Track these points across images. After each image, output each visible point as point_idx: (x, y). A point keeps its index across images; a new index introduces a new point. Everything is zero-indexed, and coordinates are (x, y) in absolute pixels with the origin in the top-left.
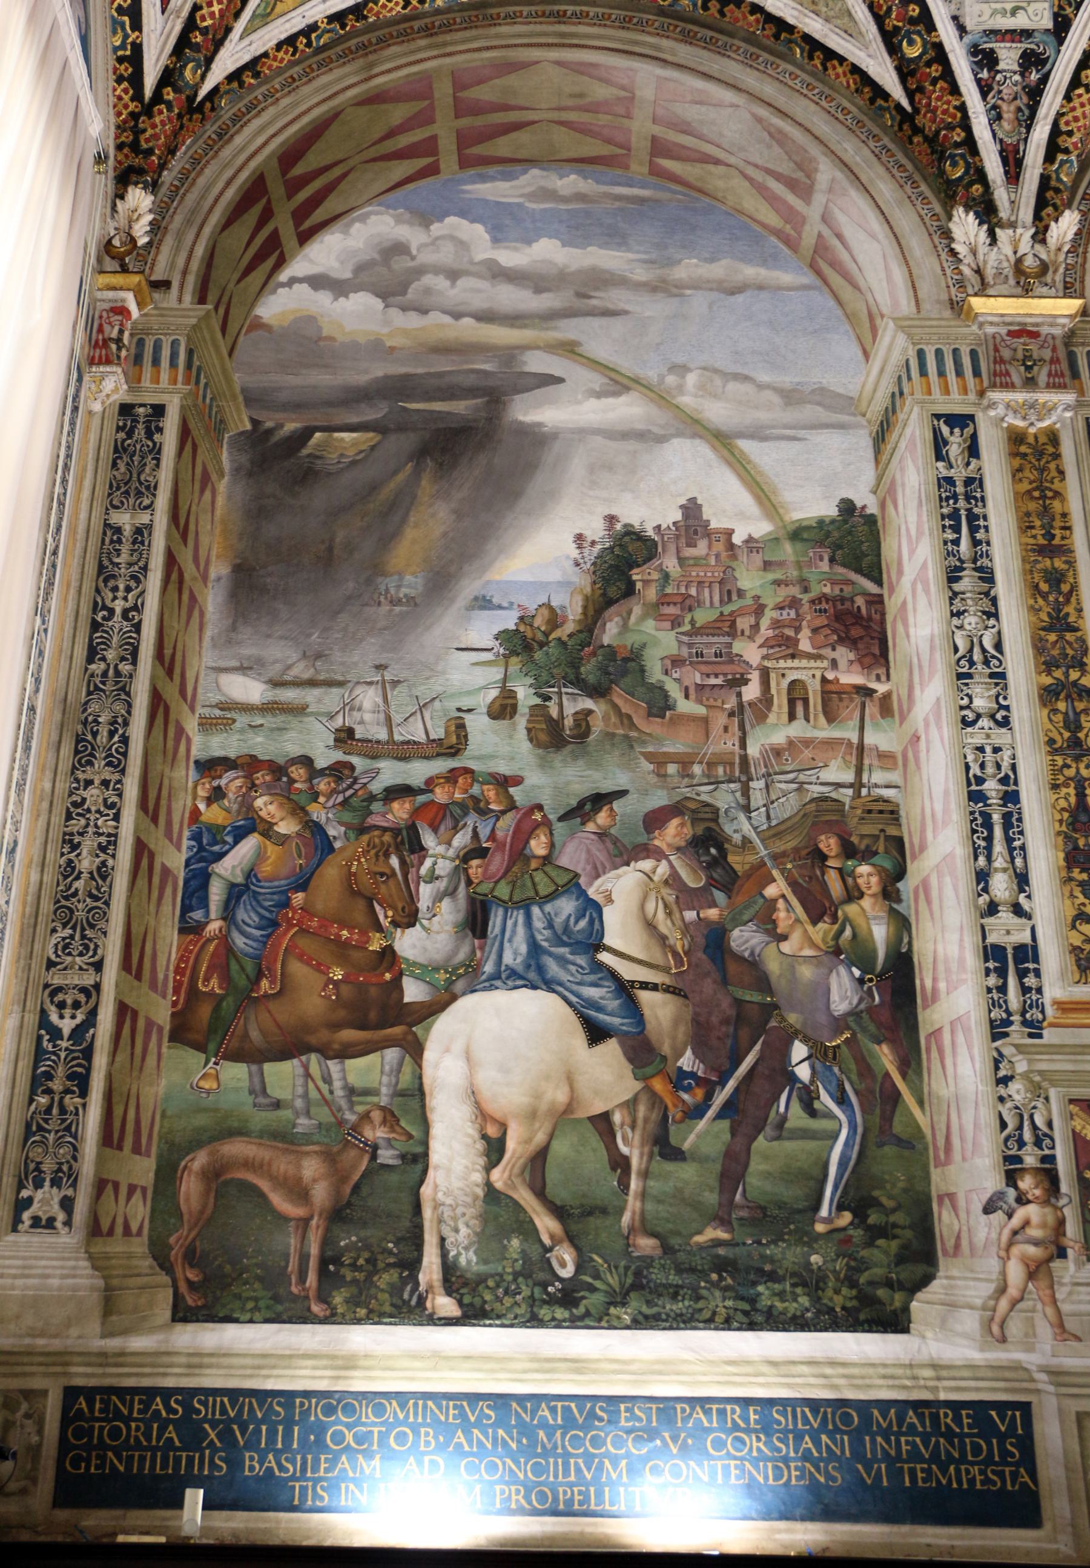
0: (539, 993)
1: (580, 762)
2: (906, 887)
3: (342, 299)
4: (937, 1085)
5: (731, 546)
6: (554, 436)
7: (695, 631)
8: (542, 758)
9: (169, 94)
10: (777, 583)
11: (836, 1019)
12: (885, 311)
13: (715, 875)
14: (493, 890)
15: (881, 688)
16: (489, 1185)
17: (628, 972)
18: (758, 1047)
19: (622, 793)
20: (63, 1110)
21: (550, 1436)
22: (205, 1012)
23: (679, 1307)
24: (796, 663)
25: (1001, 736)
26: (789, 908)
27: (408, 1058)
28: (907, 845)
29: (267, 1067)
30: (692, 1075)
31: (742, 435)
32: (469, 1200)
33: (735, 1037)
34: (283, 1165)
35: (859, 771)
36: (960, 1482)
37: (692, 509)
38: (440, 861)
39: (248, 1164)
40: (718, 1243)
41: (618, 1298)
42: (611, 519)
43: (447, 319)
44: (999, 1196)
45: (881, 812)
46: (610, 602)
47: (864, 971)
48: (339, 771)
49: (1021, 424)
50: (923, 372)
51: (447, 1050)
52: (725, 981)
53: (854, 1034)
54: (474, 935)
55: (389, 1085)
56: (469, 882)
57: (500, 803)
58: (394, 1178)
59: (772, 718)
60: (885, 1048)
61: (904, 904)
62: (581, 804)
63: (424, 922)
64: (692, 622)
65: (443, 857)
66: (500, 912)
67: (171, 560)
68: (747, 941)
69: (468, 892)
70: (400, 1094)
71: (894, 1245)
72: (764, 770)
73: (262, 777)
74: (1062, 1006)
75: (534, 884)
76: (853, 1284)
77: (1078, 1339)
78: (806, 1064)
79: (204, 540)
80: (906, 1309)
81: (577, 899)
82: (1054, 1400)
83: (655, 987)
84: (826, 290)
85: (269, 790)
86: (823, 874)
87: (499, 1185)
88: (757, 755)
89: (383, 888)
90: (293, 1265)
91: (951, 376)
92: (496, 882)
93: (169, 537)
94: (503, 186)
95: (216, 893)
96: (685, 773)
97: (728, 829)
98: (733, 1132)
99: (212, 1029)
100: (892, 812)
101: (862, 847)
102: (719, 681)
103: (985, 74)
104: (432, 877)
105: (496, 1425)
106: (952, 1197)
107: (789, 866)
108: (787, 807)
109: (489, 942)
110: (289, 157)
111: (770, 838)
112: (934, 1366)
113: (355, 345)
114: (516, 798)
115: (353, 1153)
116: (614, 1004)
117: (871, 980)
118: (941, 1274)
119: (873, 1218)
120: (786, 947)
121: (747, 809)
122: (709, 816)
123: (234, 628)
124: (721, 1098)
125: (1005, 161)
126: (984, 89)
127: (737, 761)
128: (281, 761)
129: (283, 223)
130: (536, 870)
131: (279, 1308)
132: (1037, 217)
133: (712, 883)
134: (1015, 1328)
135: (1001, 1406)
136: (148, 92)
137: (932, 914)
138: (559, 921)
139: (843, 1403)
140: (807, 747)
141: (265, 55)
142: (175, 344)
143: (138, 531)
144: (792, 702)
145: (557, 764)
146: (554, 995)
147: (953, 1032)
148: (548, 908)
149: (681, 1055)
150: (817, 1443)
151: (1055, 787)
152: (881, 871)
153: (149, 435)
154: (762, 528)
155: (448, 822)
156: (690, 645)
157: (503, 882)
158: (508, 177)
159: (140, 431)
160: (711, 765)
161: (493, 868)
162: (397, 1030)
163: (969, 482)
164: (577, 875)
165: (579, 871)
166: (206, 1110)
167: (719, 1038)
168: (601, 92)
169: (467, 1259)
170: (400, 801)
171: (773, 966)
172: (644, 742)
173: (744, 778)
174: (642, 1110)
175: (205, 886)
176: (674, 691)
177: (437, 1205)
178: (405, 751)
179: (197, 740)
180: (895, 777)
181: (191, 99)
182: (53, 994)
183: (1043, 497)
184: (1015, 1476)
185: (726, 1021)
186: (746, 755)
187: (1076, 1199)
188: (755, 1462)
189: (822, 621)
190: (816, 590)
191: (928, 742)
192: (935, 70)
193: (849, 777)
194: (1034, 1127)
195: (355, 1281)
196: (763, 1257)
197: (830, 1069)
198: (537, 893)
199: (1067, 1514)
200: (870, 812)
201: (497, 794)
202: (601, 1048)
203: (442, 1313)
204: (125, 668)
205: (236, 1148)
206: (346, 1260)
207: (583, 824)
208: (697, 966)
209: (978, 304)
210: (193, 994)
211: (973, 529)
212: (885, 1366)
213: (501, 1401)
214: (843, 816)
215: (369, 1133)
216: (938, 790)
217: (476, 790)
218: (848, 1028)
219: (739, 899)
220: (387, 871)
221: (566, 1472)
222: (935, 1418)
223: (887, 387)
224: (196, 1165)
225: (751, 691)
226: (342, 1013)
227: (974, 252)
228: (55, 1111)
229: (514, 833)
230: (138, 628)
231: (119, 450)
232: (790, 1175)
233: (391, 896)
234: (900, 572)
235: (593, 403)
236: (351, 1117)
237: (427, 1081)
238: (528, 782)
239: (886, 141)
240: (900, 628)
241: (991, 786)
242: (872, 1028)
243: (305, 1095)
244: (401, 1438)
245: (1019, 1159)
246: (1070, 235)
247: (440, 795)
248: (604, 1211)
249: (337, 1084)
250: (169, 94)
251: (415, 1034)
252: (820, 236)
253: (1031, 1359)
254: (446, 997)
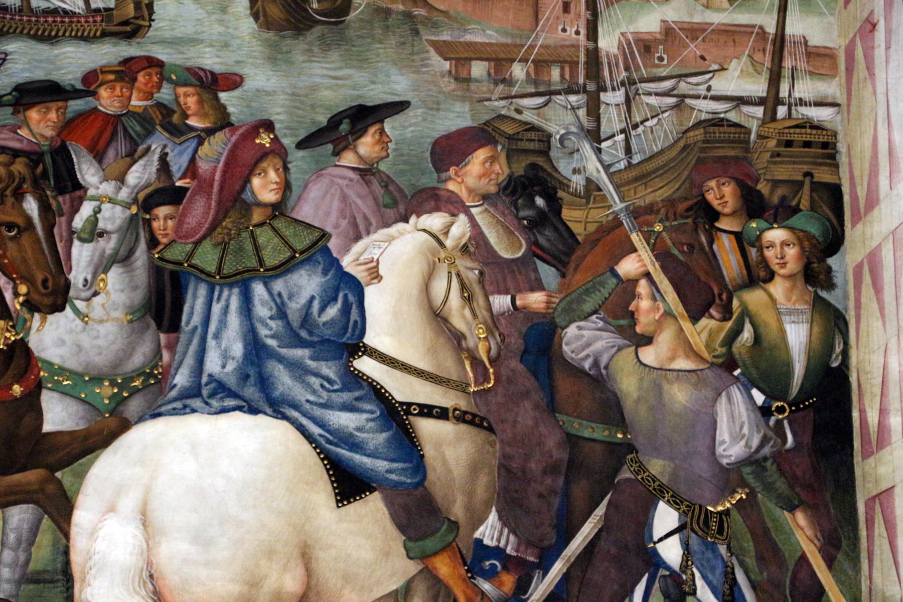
0: (261, 420)
1: (334, 55)
8: (274, 47)
11: (725, 470)
13: (542, 240)
14: (191, 255)
18: (600, 511)
19: (399, 107)
26: (656, 293)
27: (46, 522)
28: (846, 198)
30: (498, 552)
33: (566, 495)
38: (106, 207)
45: (807, 144)
47: (770, 396)
51: (112, 509)
52: (552, 407)
53: (752, 494)
54: (159, 326)
55: (13, 565)
56: (153, 242)
57: (203, 116)
60: (801, 518)
61: (838, 292)
62: (335, 122)
63: (80, 304)
65: (111, 201)
66: (203, 290)
68: (588, 345)
69: (151, 258)
72: (624, 74)
75: (257, 248)
78: (675, 539)
81: (325, 273)
83: (442, 414)
86: (711, 242)
88: (614, 50)
89: (11, 245)
92: (197, 243)
96: (500, 78)
97: (564, 167)
100: (825, 145)
101: (775, 200)
104: (93, 233)
107: (658, 228)
109: (183, 337)
111: (628, 183)
114: (230, 109)
116: (378, 439)
117: (781, 410)
120: (649, 355)
121: (595, 136)
122: (531, 146)
127: (582, 58)
130: (261, 225)
133: (536, 252)
137: (882, 309)
138: (294, 307)
140: (694, 39)
145: (298, 56)
146: (285, 424)
148: (279, 285)
149: (481, 521)
152: (802, 238)
155: (121, 146)
157: (207, 245)
160: (541, 65)
161: (192, 221)
162: (32, 476)
164: (324, 236)
165: (328, 229)
167: (541, 496)
170: (41, 108)
172: (435, 26)
173: (591, 87)
180: (831, 89)
185: (552, 469)
186: (596, 50)
191: (889, 32)
193: (758, 87)
197: (713, 547)
198: (261, 262)
200: (789, 144)
201: (200, 102)
202: (355, 508)
207: (337, 153)
208: (509, 381)
214: (747, 150)
217: (165, 94)
218: (744, 484)
219: (578, 279)
220: (20, 221)
229: (227, 164)
233: (24, 260)
237: (76, 558)
238: (248, 84)
242: (781, 485)
251: (59, 483)
254: (113, 423)
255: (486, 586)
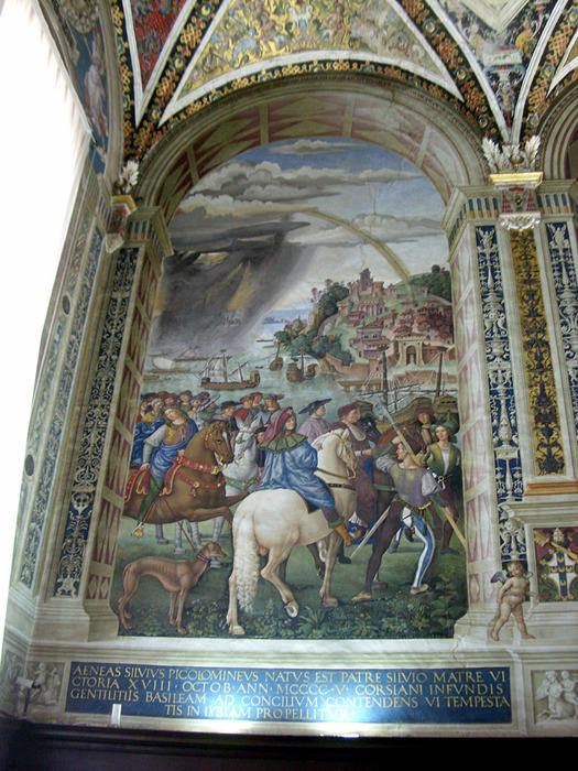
1: (310, 388)
2: (459, 435)
3: (216, 199)
4: (469, 524)
5: (382, 289)
6: (305, 247)
7: (365, 327)
9: (145, 123)
10: (403, 304)
12: (455, 184)
15: (450, 347)
16: (260, 576)
17: (328, 480)
19: (330, 400)
20: (77, 546)
21: (283, 686)
22: (139, 502)
23: (345, 630)
24: (411, 338)
25: (505, 365)
29: (164, 526)
30: (356, 525)
31: (388, 241)
32: (250, 583)
34: (169, 568)
35: (439, 384)
36: (474, 704)
37: (366, 274)
38: (245, 435)
39: (154, 568)
40: (364, 600)
41: (317, 626)
42: (328, 281)
43: (260, 203)
44: (499, 574)
46: (327, 317)
48: (203, 397)
49: (516, 228)
50: (471, 209)
52: (373, 482)
58: (217, 574)
59: (399, 363)
62: (310, 405)
64: (364, 323)
67: (137, 312)
70: (220, 536)
71: (448, 599)
73: (168, 401)
74: (533, 486)
76: (427, 617)
77: (533, 637)
79: (151, 302)
80: (452, 627)
82: (521, 666)
83: (340, 486)
84: (428, 179)
85: (172, 406)
87: (264, 576)
90: (171, 612)
91: (484, 210)
93: (136, 301)
94: (287, 147)
95: (146, 451)
98: (374, 550)
99: (142, 509)
102: (375, 348)
103: (494, 83)
104: (241, 441)
105: (259, 681)
106: (476, 576)
108: (403, 403)
110: (196, 146)
112: (464, 652)
113: (220, 217)
115: (200, 563)
116: (321, 494)
118: (470, 610)
119: (438, 586)
120: (401, 465)
121: (386, 404)
123: (161, 338)
124: (369, 534)
125: (506, 119)
126: (495, 90)
128: (178, 393)
129: (193, 171)
131: (164, 630)
132: (521, 140)
133: (368, 438)
134: (502, 634)
135: (495, 670)
136: (137, 124)
139: (421, 670)
141: (189, 106)
142: (145, 223)
143: (124, 300)
144: (408, 356)
147: (479, 500)
148: (293, 452)
150: (407, 689)
151: (531, 386)
152: (447, 428)
153: (131, 261)
154: (397, 280)
156: (362, 333)
158: (289, 144)
159: (128, 258)
163: (492, 254)
164: (306, 438)
166: (137, 544)
168: (333, 107)
169: (248, 609)
171: (396, 475)
174: (332, 541)
175: (141, 449)
176: (354, 353)
177: (236, 586)
178: (233, 387)
179: (142, 386)
180: (455, 386)
181: (156, 125)
182: (75, 496)
183: (526, 259)
184: (500, 701)
187: (535, 573)
188: (377, 697)
189: (424, 319)
190: (421, 306)
192: (472, 83)
194: (517, 542)
195: (198, 619)
196: (385, 605)
199: (524, 716)
203: (236, 633)
204: (114, 357)
205: (149, 561)
206: (194, 610)
209: (494, 177)
210: (134, 494)
211: (494, 275)
212: (441, 653)
213: (261, 672)
215: (207, 555)
216: (475, 391)
219: (381, 446)
221: (290, 702)
222: (464, 676)
223: (455, 215)
224: (131, 569)
225: (390, 352)
226: (199, 502)
227: (493, 157)
228: (74, 545)
230: (120, 340)
231: (119, 268)
232: (398, 569)
234: (460, 296)
235: (322, 233)
236: (199, 547)
238: (286, 397)
239: (455, 115)
240: (459, 320)
241: (500, 388)
243: (180, 538)
244: (215, 687)
245: (509, 557)
246: (537, 146)
247: (246, 405)
248: (312, 587)
249: (194, 533)
250: (145, 123)
252: (426, 156)
253: (509, 648)
255: (352, 535)
